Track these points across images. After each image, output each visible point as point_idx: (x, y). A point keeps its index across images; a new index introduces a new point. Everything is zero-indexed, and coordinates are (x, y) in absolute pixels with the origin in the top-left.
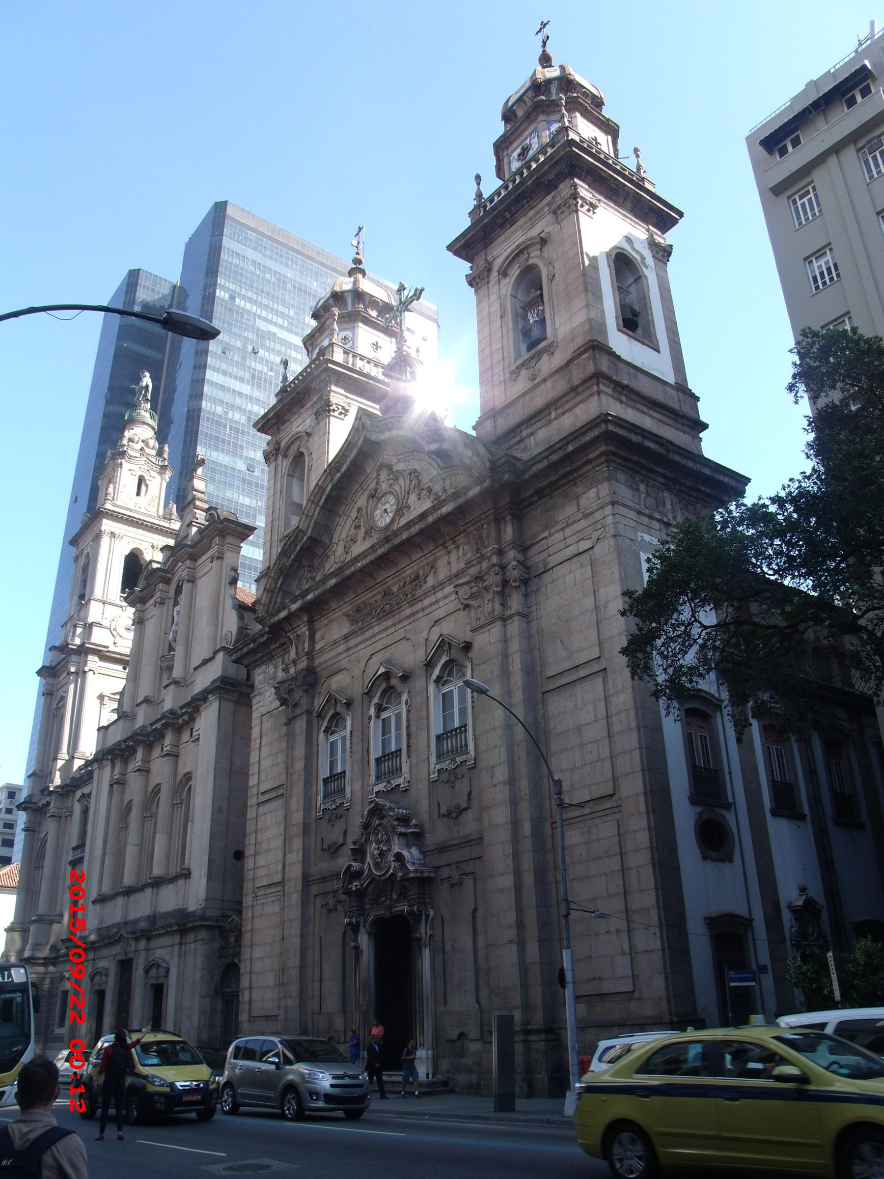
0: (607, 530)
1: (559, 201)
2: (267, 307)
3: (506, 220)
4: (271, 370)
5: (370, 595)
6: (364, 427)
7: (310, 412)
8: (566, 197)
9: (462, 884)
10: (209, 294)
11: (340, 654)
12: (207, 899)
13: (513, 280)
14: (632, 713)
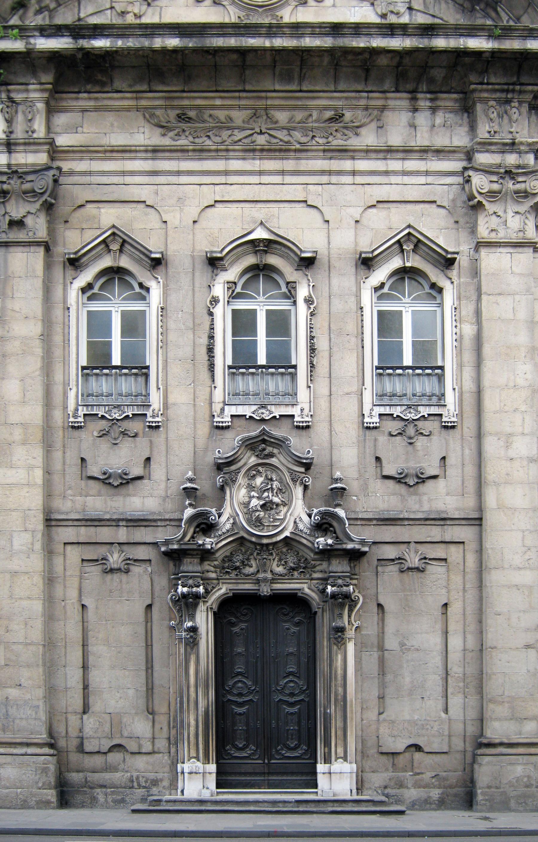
5: (218, 102)
11: (132, 173)
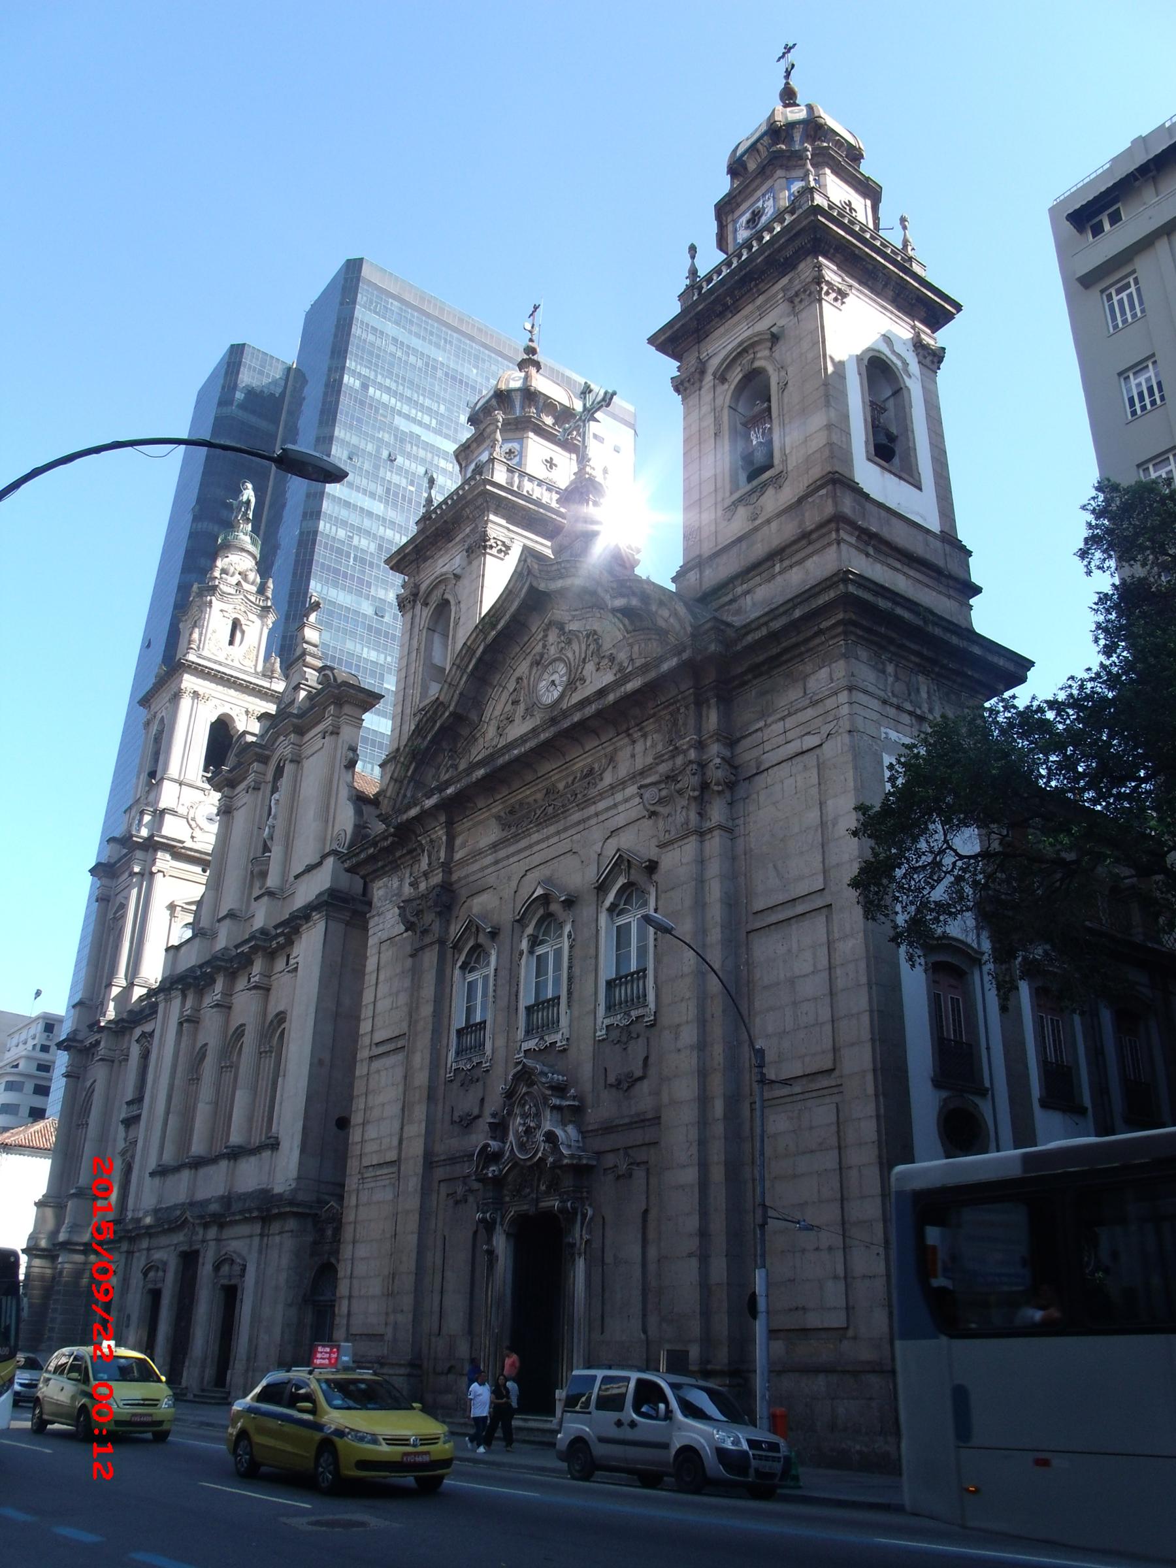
0: (841, 723)
1: (797, 286)
2: (409, 400)
3: (727, 308)
4: (412, 484)
5: (528, 792)
6: (529, 572)
7: (460, 548)
8: (807, 280)
9: (631, 1175)
10: (335, 380)
11: (487, 867)
12: (299, 1178)
13: (733, 387)
14: (863, 965)
